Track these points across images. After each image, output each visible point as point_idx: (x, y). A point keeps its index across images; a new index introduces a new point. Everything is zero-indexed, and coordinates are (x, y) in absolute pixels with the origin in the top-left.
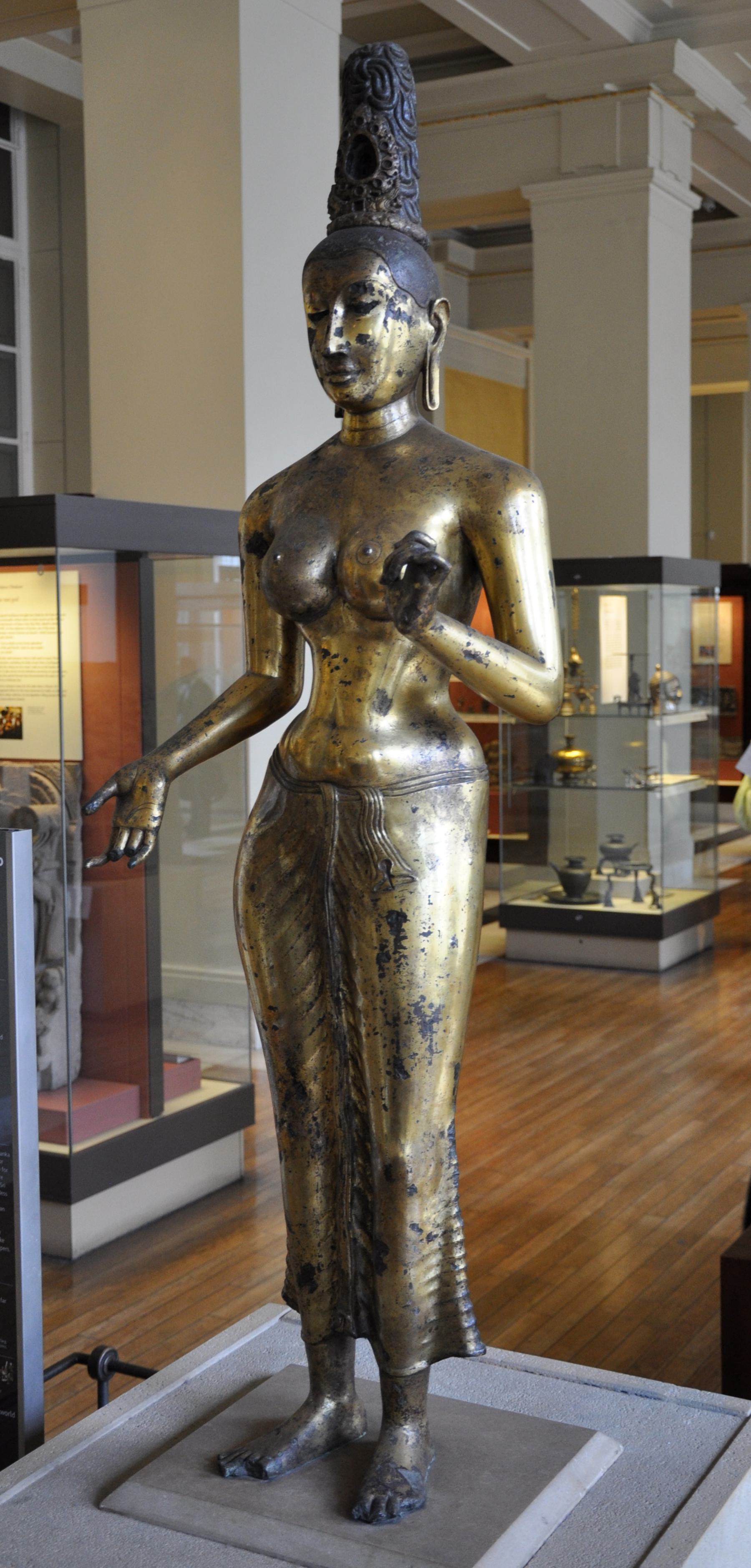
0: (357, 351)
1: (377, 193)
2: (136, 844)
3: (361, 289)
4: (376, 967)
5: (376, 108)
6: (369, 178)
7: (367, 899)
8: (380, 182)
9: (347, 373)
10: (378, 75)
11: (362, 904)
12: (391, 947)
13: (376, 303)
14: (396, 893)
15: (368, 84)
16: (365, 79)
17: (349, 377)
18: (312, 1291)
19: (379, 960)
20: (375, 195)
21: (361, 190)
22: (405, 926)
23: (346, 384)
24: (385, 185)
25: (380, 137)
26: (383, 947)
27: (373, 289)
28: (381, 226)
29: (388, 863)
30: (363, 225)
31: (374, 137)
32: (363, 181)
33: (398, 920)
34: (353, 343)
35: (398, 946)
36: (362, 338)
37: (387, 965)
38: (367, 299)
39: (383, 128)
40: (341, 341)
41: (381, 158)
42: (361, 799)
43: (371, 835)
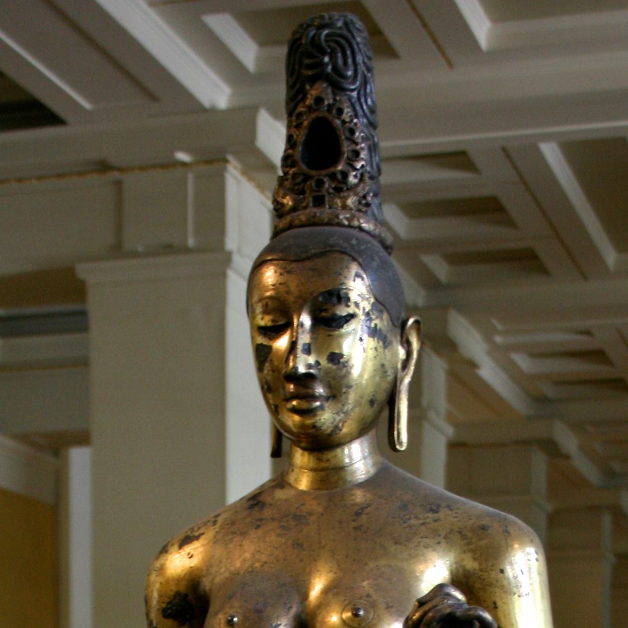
0: (327, 372)
1: (341, 186)
3: (335, 299)
5: (338, 88)
6: (332, 170)
8: (345, 175)
9: (314, 398)
13: (352, 316)
17: (318, 404)
20: (338, 190)
21: (320, 183)
24: (352, 180)
25: (344, 122)
27: (348, 299)
28: (350, 226)
30: (329, 224)
31: (338, 122)
32: (324, 172)
34: (324, 362)
36: (335, 358)
38: (342, 311)
39: (347, 112)
40: (311, 360)
41: (346, 147)
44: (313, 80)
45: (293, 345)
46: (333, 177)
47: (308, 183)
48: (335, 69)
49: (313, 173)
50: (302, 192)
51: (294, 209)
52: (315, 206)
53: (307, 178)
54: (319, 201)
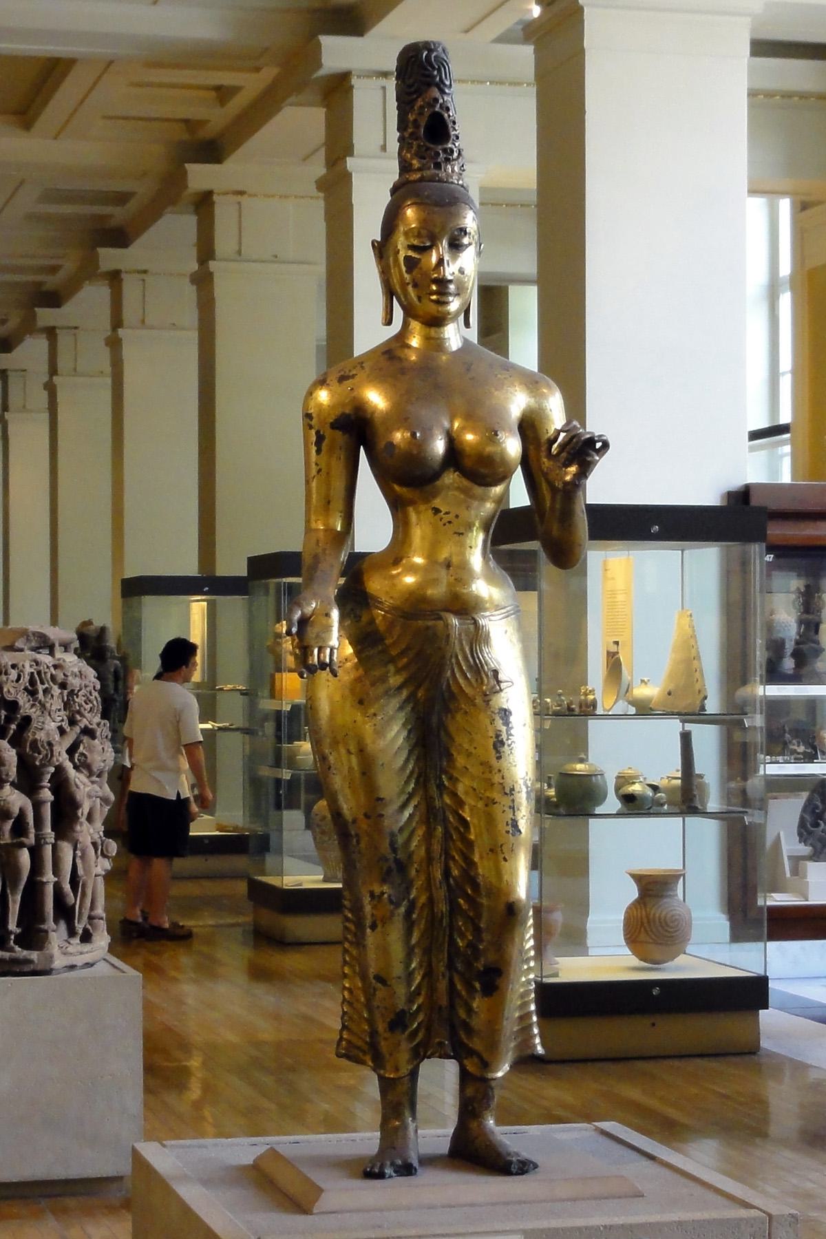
2: (328, 660)
4: (494, 752)
5: (443, 92)
7: (479, 701)
8: (452, 151)
11: (475, 705)
12: (504, 736)
13: (470, 244)
14: (502, 694)
18: (403, 1032)
19: (495, 747)
20: (447, 160)
22: (512, 719)
23: (447, 303)
26: (498, 736)
29: (496, 672)
33: (505, 714)
35: (509, 735)
37: (502, 749)
42: (475, 623)
43: (481, 651)
44: (429, 85)
45: (441, 262)
46: (445, 151)
51: (420, 169)
54: (438, 166)
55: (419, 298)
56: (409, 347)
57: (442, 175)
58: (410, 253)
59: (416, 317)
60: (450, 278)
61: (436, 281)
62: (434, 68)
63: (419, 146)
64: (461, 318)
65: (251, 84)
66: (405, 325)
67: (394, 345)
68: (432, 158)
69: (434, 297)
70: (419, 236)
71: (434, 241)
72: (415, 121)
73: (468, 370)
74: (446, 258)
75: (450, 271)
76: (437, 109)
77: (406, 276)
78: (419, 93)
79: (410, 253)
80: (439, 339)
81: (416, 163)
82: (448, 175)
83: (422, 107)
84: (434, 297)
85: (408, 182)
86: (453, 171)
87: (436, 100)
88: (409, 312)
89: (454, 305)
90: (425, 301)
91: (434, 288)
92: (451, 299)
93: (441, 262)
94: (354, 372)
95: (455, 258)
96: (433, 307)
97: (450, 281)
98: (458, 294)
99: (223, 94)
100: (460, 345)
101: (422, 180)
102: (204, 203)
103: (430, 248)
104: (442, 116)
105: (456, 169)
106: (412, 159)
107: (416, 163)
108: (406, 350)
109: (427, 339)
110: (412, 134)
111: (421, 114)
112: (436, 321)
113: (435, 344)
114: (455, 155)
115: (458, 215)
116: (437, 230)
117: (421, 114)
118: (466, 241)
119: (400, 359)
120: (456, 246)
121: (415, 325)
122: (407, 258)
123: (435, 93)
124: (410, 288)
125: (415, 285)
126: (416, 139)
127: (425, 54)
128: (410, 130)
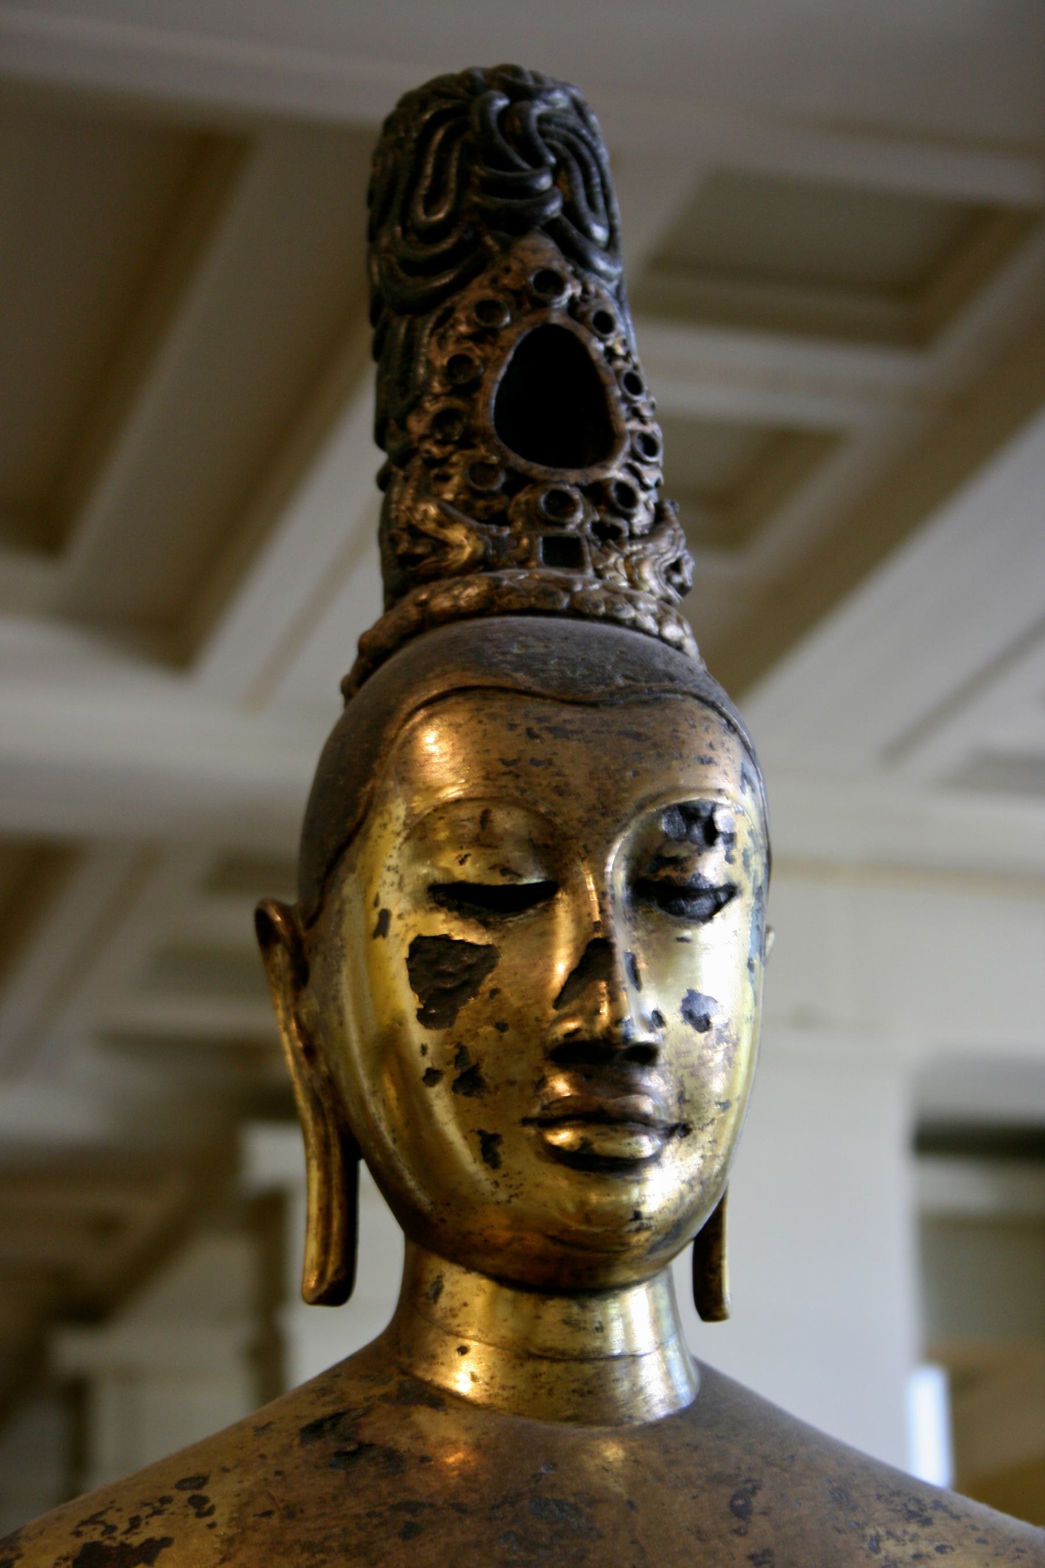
3: (697, 831)
5: (582, 262)
6: (597, 474)
8: (627, 497)
9: (646, 1123)
10: (574, 165)
13: (731, 891)
15: (545, 182)
16: (537, 162)
20: (608, 535)
21: (562, 504)
23: (630, 1167)
25: (610, 353)
32: (574, 476)
34: (673, 1016)
44: (520, 223)
45: (595, 958)
46: (596, 493)
47: (522, 497)
48: (570, 209)
49: (538, 470)
50: (502, 519)
51: (479, 564)
52: (551, 560)
53: (518, 481)
54: (566, 553)
55: (488, 1147)
56: (442, 1399)
57: (586, 583)
58: (443, 925)
59: (468, 1255)
60: (642, 1036)
61: (570, 1054)
62: (537, 162)
63: (480, 471)
64: (683, 1265)
65: (145, 1210)
66: (417, 1296)
67: (356, 1394)
68: (534, 519)
69: (563, 1137)
70: (483, 838)
71: (560, 853)
72: (459, 362)
73: (741, 1512)
74: (624, 940)
75: (645, 1006)
76: (556, 318)
77: (418, 1035)
78: (471, 261)
79: (443, 925)
80: (584, 1357)
81: (463, 541)
82: (614, 591)
83: (487, 309)
84: (563, 1137)
85: (430, 621)
86: (635, 583)
87: (553, 282)
88: (431, 1236)
89: (662, 1186)
90: (521, 1160)
91: (561, 1086)
92: (646, 1145)
93: (595, 958)
94: (153, 1529)
95: (669, 949)
96: (559, 1188)
97: (647, 1055)
98: (682, 1129)
99: (106, 1227)
100: (685, 1393)
101: (485, 608)
102: (77, 1395)
103: (543, 896)
104: (583, 351)
105: (651, 578)
106: (445, 520)
107: (463, 541)
108: (423, 1417)
109: (521, 1354)
110: (443, 419)
111: (485, 334)
112: (572, 1266)
113: (569, 1382)
114: (642, 518)
115: (669, 749)
116: (573, 811)
117: (485, 334)
118: (712, 868)
119: (393, 1460)
120: (669, 894)
121: (468, 1293)
122: (425, 954)
123: (545, 252)
124: (441, 1102)
125: (468, 1082)
126: (466, 442)
127: (502, 103)
128: (432, 407)
